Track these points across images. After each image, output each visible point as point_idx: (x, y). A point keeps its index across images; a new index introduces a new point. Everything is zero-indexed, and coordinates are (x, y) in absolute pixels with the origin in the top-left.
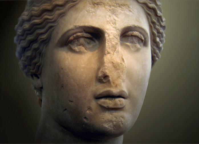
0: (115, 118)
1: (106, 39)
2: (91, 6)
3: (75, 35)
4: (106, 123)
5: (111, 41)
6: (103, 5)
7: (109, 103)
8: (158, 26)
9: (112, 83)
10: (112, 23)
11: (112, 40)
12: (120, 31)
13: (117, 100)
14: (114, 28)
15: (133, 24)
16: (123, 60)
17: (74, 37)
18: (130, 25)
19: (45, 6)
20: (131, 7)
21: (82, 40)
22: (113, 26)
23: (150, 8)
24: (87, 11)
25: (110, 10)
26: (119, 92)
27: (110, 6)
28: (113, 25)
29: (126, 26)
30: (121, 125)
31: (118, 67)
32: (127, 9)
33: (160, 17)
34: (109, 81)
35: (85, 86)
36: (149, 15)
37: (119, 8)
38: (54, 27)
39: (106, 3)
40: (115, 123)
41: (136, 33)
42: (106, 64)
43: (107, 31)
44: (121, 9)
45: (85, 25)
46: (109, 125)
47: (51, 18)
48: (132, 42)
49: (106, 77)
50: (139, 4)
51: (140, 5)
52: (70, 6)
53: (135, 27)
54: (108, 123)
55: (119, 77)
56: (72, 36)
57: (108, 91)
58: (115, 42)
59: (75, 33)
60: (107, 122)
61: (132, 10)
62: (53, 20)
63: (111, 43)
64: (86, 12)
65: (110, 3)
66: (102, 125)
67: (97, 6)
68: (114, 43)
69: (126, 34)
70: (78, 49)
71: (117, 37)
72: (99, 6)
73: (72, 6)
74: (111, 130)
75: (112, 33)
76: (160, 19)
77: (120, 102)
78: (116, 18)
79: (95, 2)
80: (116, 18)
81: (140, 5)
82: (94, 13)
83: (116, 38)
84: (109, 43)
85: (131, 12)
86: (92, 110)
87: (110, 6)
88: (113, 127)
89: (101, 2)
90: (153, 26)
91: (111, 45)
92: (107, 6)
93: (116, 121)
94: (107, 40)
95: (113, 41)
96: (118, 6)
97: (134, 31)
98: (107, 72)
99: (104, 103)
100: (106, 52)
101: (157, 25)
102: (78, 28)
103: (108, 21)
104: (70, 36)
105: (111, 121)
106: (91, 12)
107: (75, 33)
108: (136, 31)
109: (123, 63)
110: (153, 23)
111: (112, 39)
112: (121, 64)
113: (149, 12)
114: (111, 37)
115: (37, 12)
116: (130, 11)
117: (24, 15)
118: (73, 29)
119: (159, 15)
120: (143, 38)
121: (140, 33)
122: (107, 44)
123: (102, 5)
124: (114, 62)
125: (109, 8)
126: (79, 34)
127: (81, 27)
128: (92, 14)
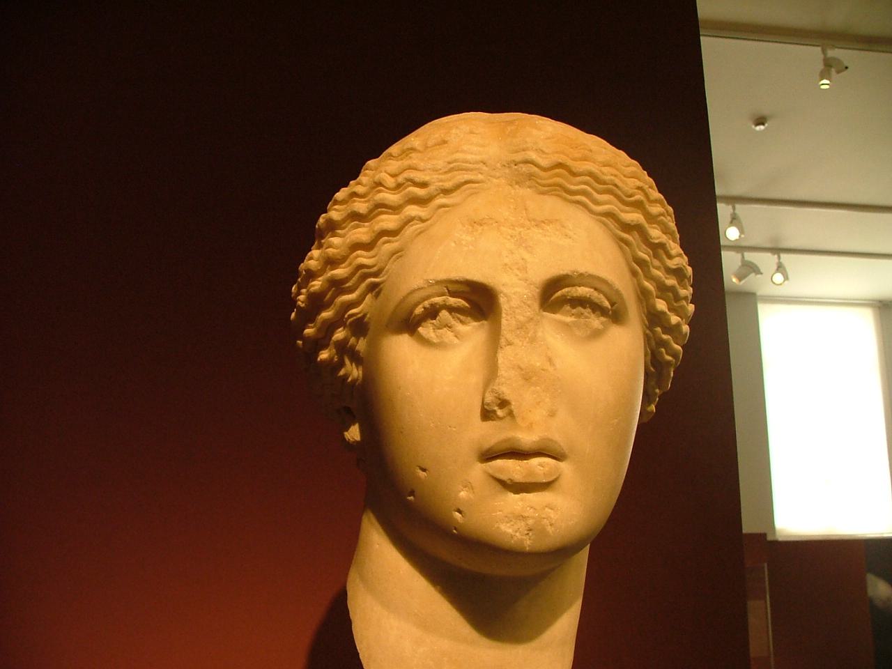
0: (532, 510)
1: (501, 310)
2: (464, 229)
3: (426, 304)
4: (508, 523)
5: (514, 312)
6: (494, 225)
7: (513, 469)
8: (657, 268)
9: (519, 420)
10: (518, 269)
11: (517, 311)
12: (537, 288)
13: (535, 461)
14: (521, 282)
16: (550, 360)
17: (424, 308)
18: (565, 273)
19: (358, 236)
21: (444, 314)
22: (520, 275)
23: (627, 227)
24: (455, 242)
25: (511, 236)
27: (513, 226)
28: (521, 273)
29: (554, 275)
30: (550, 529)
31: (534, 378)
32: (557, 230)
33: (662, 246)
34: (511, 414)
35: (455, 428)
36: (627, 243)
37: (535, 230)
38: (382, 286)
39: (503, 220)
40: (530, 522)
41: (582, 291)
42: (503, 372)
43: (505, 290)
44: (541, 231)
45: (450, 277)
46: (516, 527)
47: (371, 264)
49: (503, 403)
50: (593, 216)
52: (416, 232)
54: (512, 523)
55: (538, 403)
56: (421, 306)
57: (509, 440)
58: (524, 316)
59: (428, 297)
60: (511, 521)
61: (571, 233)
62: (375, 269)
63: (515, 317)
64: (453, 245)
65: (514, 219)
66: (498, 528)
67: (480, 229)
68: (521, 318)
69: (554, 294)
70: (437, 336)
71: (529, 302)
72: (486, 228)
73: (419, 231)
74: (522, 540)
75: (516, 293)
76: (661, 252)
77: (542, 468)
78: (527, 256)
79: (476, 220)
80: (527, 256)
82: (472, 245)
83: (529, 306)
84: (509, 318)
85: (570, 238)
86: (473, 489)
87: (512, 227)
88: (526, 532)
89: (491, 218)
90: (640, 271)
91: (514, 322)
92: (504, 226)
93: (533, 518)
94: (504, 311)
97: (580, 286)
98: (507, 392)
99: (501, 470)
100: (503, 342)
101: (654, 267)
102: (432, 285)
103: (506, 265)
104: (416, 305)
105: (524, 518)
106: (464, 243)
107: (428, 297)
109: (551, 369)
110: (641, 263)
111: (517, 308)
112: (543, 370)
113: (625, 236)
114: (514, 303)
115: (338, 250)
116: (566, 235)
117: (311, 258)
118: (419, 289)
119: (657, 241)
120: (607, 304)
121: (596, 289)
122: (504, 321)
123: (492, 224)
124: (522, 366)
125: (510, 231)
126: (438, 300)
127: (438, 282)
128: (466, 249)
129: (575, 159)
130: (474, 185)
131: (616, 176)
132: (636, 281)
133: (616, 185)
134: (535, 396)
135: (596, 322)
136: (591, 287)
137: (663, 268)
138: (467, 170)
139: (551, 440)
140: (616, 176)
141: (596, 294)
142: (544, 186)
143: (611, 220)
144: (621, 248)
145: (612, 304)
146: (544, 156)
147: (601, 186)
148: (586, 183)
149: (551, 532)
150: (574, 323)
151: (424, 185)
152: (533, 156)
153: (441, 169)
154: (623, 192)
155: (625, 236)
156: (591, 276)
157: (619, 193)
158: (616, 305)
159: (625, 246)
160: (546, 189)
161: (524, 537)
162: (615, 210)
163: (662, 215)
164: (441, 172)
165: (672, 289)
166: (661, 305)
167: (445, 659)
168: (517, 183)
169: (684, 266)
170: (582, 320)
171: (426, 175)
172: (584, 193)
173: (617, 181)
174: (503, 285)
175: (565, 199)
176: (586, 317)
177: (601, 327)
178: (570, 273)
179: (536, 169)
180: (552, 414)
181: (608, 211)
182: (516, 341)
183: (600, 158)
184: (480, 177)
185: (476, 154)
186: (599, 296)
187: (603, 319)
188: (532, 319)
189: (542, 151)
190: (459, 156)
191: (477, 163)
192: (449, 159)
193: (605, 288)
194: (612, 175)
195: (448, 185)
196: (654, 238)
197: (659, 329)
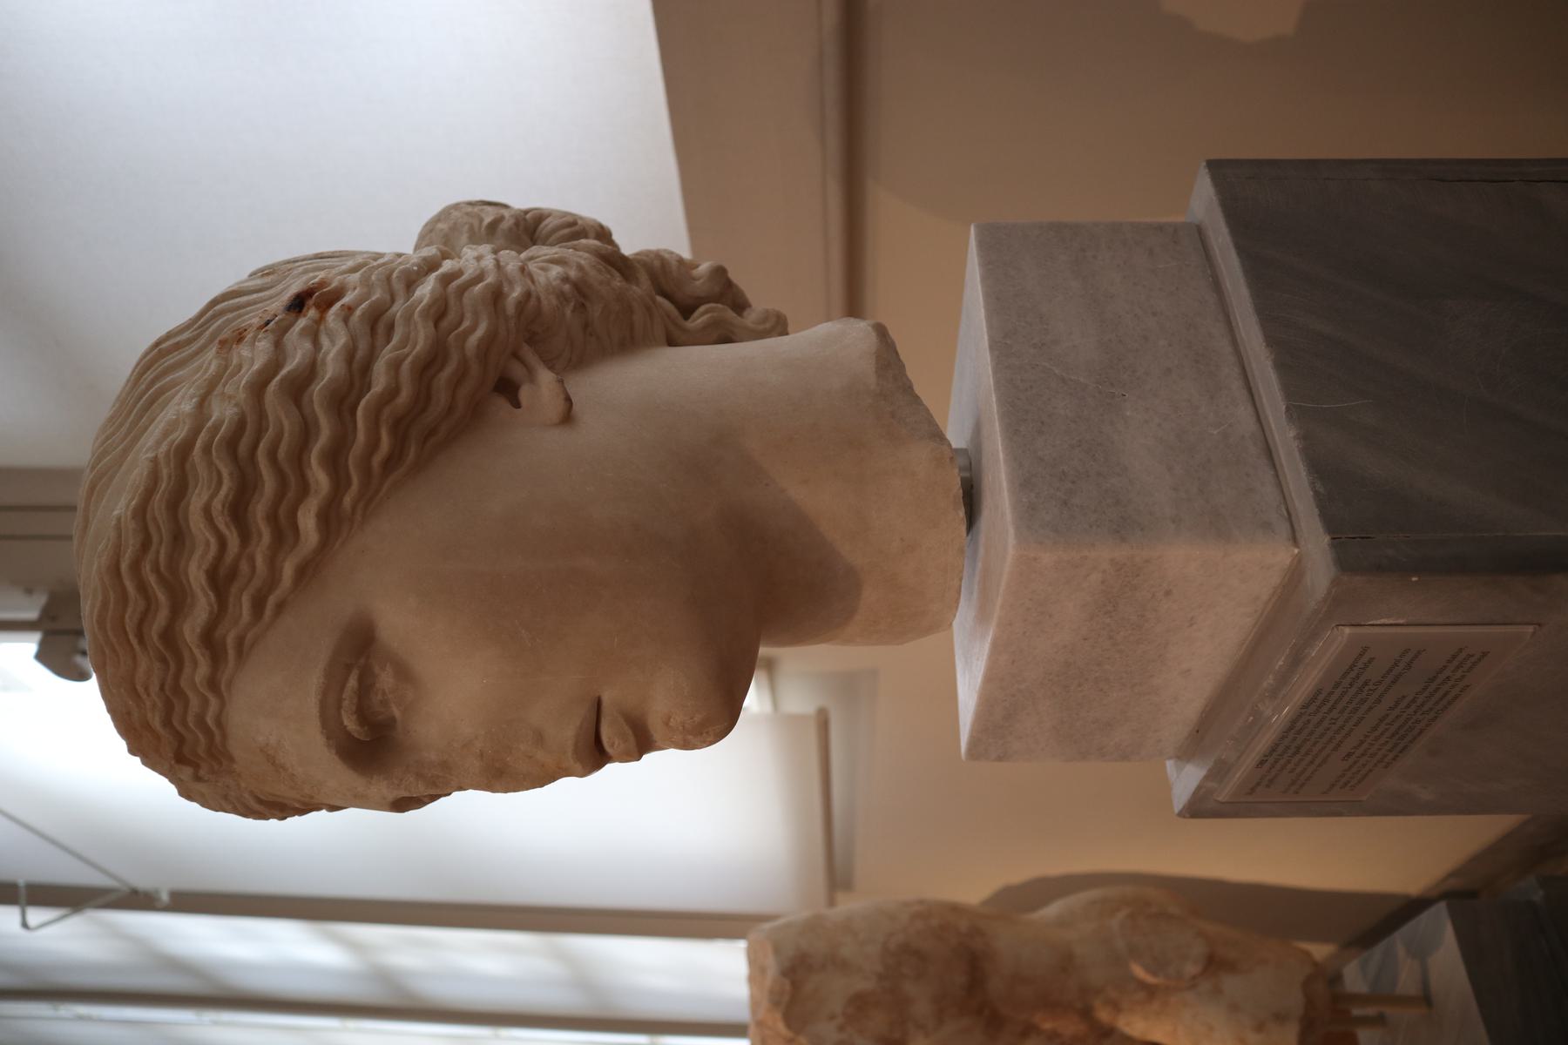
30: (698, 718)
36: (240, 642)
41: (350, 723)
53: (328, 738)
76: (222, 572)
110: (258, 605)
113: (231, 653)
120: (352, 683)
121: (339, 707)
133: (162, 688)
135: (386, 679)
136: (340, 714)
141: (346, 703)
144: (252, 645)
145: (349, 668)
155: (231, 653)
163: (156, 569)
165: (272, 518)
166: (308, 521)
172: (201, 721)
173: (154, 688)
175: (224, 736)
176: (384, 693)
187: (377, 669)
196: (210, 605)
197: (347, 501)
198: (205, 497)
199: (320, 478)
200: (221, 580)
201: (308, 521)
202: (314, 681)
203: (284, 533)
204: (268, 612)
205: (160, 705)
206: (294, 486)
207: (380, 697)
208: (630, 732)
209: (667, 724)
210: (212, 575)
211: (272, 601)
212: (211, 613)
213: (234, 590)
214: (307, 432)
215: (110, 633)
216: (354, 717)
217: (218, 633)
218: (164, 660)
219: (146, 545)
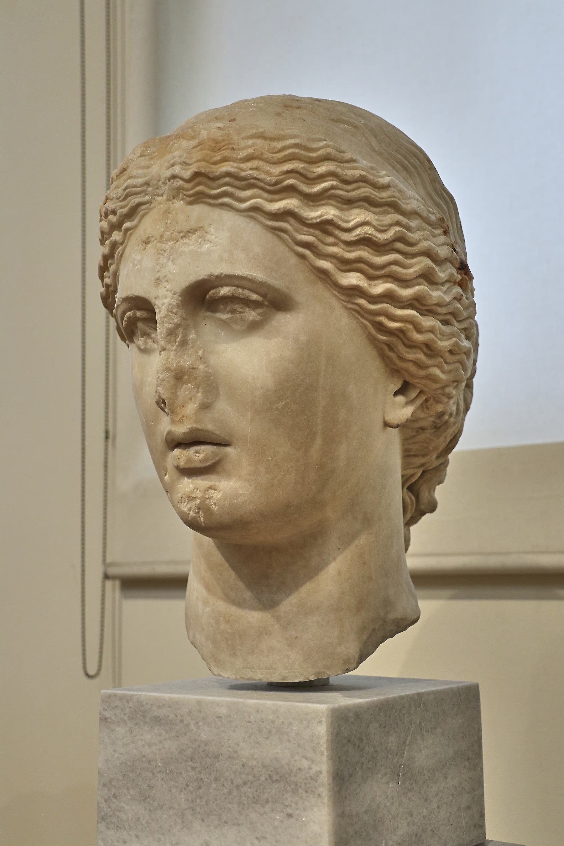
5: (163, 321)
10: (167, 281)
13: (193, 449)
15: (209, 273)
18: (201, 278)
20: (212, 230)
26: (187, 433)
30: (215, 508)
31: (186, 377)
40: (198, 502)
41: (225, 291)
43: (157, 302)
46: (189, 506)
48: (233, 311)
51: (245, 214)
53: (217, 277)
75: (165, 301)
76: (330, 228)
81: (245, 216)
95: (167, 322)
96: (182, 238)
103: (158, 279)
105: (195, 498)
106: (136, 262)
108: (226, 285)
109: (202, 367)
120: (255, 297)
121: (238, 287)
124: (172, 368)
129: (215, 163)
130: (144, 207)
131: (256, 169)
132: (308, 264)
133: (256, 179)
134: (187, 392)
135: (252, 315)
137: (340, 243)
138: (136, 194)
139: (201, 430)
140: (256, 169)
141: (240, 290)
142: (189, 196)
143: (260, 213)
144: (278, 236)
145: (264, 296)
146: (187, 167)
147: (243, 183)
148: (226, 184)
149: (215, 509)
150: (230, 319)
151: (114, 212)
152: (177, 170)
153: (120, 197)
154: (265, 183)
156: (227, 276)
157: (262, 184)
158: (268, 296)
159: (282, 234)
160: (191, 199)
161: (197, 515)
162: (256, 203)
163: (333, 188)
164: (121, 199)
165: (360, 260)
166: (353, 279)
167: (222, 619)
168: (174, 198)
169: (370, 234)
170: (238, 315)
171: (113, 204)
173: (255, 174)
174: (155, 298)
176: (240, 312)
177: (258, 318)
178: (206, 277)
179: (181, 182)
180: (205, 407)
181: (252, 206)
182: (169, 346)
183: (243, 154)
184: (147, 198)
185: (141, 178)
186: (244, 292)
187: (259, 311)
188: (179, 325)
189: (185, 163)
190: (130, 182)
191: (141, 186)
192: (123, 187)
193: (244, 283)
194: (251, 169)
195: (125, 210)
196: (312, 219)
197: (362, 301)
198: (374, 223)
199: (380, 288)
200: (325, 226)
201: (353, 279)
202: (260, 276)
203: (347, 265)
204: (300, 250)
205: (243, 174)
206: (373, 273)
207: (239, 309)
208: (207, 464)
209: (210, 488)
210: (330, 222)
211: (307, 252)
212: (306, 219)
213: (317, 232)
214: (404, 282)
215: (291, 151)
216: (230, 294)
217: (292, 221)
218: (276, 184)
219: (346, 182)
